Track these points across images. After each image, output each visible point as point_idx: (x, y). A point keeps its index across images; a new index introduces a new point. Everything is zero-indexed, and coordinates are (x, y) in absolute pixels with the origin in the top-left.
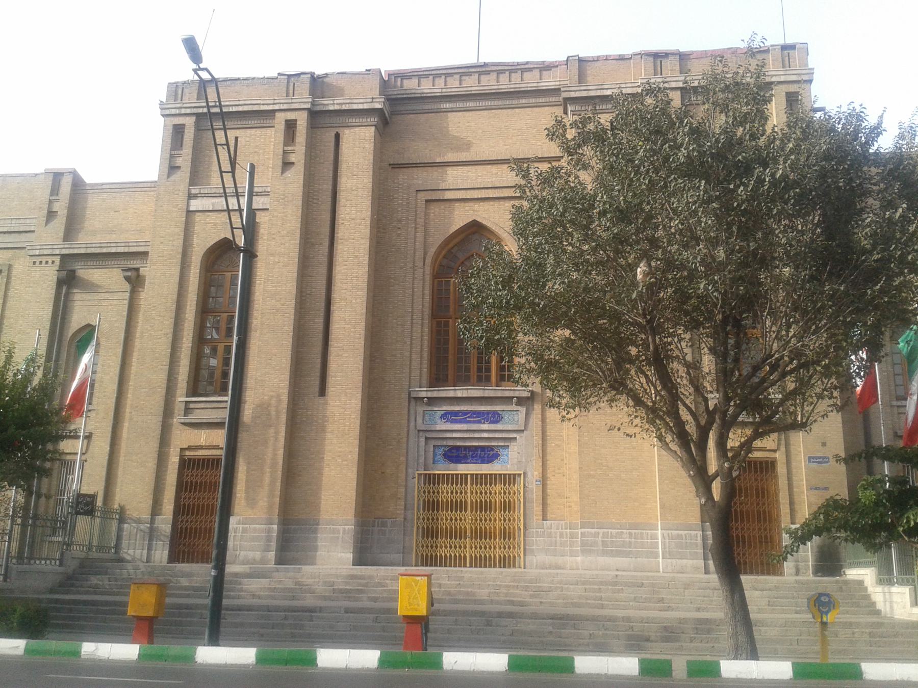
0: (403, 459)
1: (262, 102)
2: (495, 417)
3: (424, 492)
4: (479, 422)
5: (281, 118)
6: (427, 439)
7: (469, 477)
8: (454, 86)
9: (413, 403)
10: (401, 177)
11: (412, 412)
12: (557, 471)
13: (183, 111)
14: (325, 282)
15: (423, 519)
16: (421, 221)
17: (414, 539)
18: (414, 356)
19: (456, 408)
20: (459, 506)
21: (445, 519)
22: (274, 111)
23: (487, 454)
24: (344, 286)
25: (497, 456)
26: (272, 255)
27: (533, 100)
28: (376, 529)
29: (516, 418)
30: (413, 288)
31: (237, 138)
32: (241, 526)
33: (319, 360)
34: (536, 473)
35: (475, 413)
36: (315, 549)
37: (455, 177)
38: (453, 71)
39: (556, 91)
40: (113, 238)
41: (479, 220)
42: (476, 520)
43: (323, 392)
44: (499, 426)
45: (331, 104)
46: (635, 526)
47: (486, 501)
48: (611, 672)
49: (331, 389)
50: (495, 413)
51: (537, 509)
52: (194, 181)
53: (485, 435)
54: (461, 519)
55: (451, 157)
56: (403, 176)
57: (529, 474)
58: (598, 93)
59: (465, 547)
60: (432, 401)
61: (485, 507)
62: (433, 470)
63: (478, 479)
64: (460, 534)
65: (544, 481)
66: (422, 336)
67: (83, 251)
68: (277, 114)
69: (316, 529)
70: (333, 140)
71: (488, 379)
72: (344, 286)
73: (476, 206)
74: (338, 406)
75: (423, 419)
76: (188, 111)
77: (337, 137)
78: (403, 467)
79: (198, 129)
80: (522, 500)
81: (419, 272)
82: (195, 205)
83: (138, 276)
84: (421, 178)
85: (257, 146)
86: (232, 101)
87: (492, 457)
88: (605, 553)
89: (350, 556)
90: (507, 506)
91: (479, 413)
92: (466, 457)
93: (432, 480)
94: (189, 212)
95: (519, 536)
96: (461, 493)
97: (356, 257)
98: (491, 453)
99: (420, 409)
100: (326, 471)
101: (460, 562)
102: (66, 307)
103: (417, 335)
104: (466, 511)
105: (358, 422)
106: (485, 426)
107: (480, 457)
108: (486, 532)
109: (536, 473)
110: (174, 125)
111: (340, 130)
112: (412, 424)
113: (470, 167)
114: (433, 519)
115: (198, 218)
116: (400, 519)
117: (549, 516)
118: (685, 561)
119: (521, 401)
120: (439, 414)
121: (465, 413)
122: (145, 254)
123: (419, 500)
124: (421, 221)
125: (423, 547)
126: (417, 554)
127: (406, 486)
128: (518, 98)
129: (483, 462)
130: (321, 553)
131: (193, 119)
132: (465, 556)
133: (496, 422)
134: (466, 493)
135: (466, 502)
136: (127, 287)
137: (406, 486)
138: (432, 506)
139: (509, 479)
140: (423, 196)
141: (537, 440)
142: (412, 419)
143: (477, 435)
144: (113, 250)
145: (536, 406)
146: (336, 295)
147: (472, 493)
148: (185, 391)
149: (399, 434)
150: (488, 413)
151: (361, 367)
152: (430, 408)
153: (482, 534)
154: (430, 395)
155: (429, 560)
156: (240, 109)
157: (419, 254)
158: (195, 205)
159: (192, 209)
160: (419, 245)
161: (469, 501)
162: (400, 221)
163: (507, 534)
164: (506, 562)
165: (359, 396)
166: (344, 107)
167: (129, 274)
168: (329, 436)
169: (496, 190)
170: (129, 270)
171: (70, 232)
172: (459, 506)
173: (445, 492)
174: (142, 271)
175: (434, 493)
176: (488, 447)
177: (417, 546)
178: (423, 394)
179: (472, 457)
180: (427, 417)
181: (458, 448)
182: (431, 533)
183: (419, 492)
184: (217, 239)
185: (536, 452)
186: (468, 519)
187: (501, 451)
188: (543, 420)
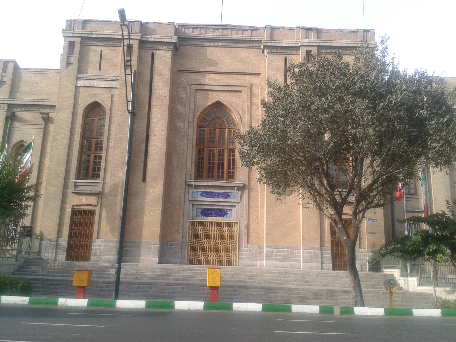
0: (182, 214)
1: (115, 34)
2: (226, 196)
3: (192, 230)
4: (219, 198)
6: (193, 204)
8: (210, 34)
9: (187, 187)
10: (183, 77)
11: (187, 191)
12: (255, 222)
13: (75, 35)
14: (146, 126)
15: (191, 242)
16: (193, 99)
17: (186, 252)
18: (188, 165)
19: (208, 191)
20: (208, 237)
21: (202, 242)
23: (221, 213)
24: (156, 129)
25: (226, 214)
27: (247, 45)
28: (168, 247)
29: (236, 196)
30: (188, 132)
31: (101, 51)
32: (103, 244)
33: (143, 165)
34: (245, 222)
35: (216, 193)
36: (140, 255)
37: (209, 79)
38: (210, 27)
39: (260, 42)
40: (35, 97)
41: (220, 100)
42: (216, 243)
43: (144, 180)
44: (228, 200)
45: (150, 38)
46: (290, 248)
47: (221, 235)
48: (307, 312)
49: (148, 179)
50: (226, 193)
51: (245, 239)
52: (79, 71)
53: (221, 204)
54: (209, 243)
55: (208, 69)
56: (184, 77)
57: (242, 223)
58: (280, 45)
59: (211, 256)
60: (197, 187)
61: (219, 237)
62: (196, 219)
63: (218, 224)
64: (208, 250)
65: (248, 226)
66: (192, 155)
67: (19, 103)
69: (140, 246)
70: (151, 56)
71: (222, 177)
72: (156, 129)
73: (219, 94)
74: (152, 187)
76: (77, 35)
77: (153, 54)
78: (182, 218)
79: (82, 45)
80: (238, 235)
81: (191, 124)
82: (80, 83)
83: (48, 117)
84: (193, 78)
86: (97, 32)
87: (224, 214)
88: (276, 260)
89: (157, 259)
90: (230, 237)
91: (219, 194)
92: (211, 214)
93: (195, 224)
94: (76, 86)
95: (236, 251)
96: (209, 230)
98: (224, 212)
99: (191, 190)
100: (145, 218)
101: (207, 262)
102: (10, 131)
103: (190, 154)
104: (211, 239)
105: (162, 195)
106: (221, 200)
108: (220, 249)
109: (245, 222)
110: (70, 42)
111: (154, 51)
112: (187, 197)
113: (217, 75)
114: (196, 243)
115: (81, 90)
116: (180, 242)
117: (250, 242)
118: (312, 264)
119: (239, 188)
120: (200, 193)
121: (212, 193)
122: (53, 107)
123: (189, 233)
124: (193, 99)
125: (190, 255)
126: (188, 259)
127: (183, 227)
128: (241, 43)
129: (219, 216)
130: (142, 258)
131: (80, 39)
132: (210, 260)
133: (227, 198)
134: (212, 231)
135: (211, 235)
136: (43, 122)
137: (183, 227)
138: (195, 236)
139: (231, 225)
140: (194, 87)
141: (246, 207)
142: (187, 195)
143: (217, 204)
144: (36, 103)
145: (245, 191)
146: (151, 133)
147: (214, 231)
148: (74, 177)
149: (180, 202)
150: (223, 193)
151: (163, 169)
152: (195, 190)
153: (218, 250)
154: (196, 184)
155: (192, 262)
156: (104, 36)
157: (192, 115)
158: (80, 83)
159: (78, 85)
160: (191, 111)
161: (213, 234)
162: (182, 98)
163: (229, 250)
164: (228, 263)
165: (162, 183)
166: (157, 40)
167: (44, 116)
168: (147, 201)
169: (229, 87)
170: (44, 114)
171: (12, 93)
172: (208, 237)
173: (201, 230)
174: (50, 115)
175: (196, 230)
176: (222, 209)
177: (188, 255)
178: (193, 183)
179: (214, 214)
180: (194, 194)
181: (208, 209)
182: (194, 249)
183: (189, 229)
184: (91, 101)
185: (245, 212)
186: (212, 243)
187: (228, 212)
188: (249, 198)
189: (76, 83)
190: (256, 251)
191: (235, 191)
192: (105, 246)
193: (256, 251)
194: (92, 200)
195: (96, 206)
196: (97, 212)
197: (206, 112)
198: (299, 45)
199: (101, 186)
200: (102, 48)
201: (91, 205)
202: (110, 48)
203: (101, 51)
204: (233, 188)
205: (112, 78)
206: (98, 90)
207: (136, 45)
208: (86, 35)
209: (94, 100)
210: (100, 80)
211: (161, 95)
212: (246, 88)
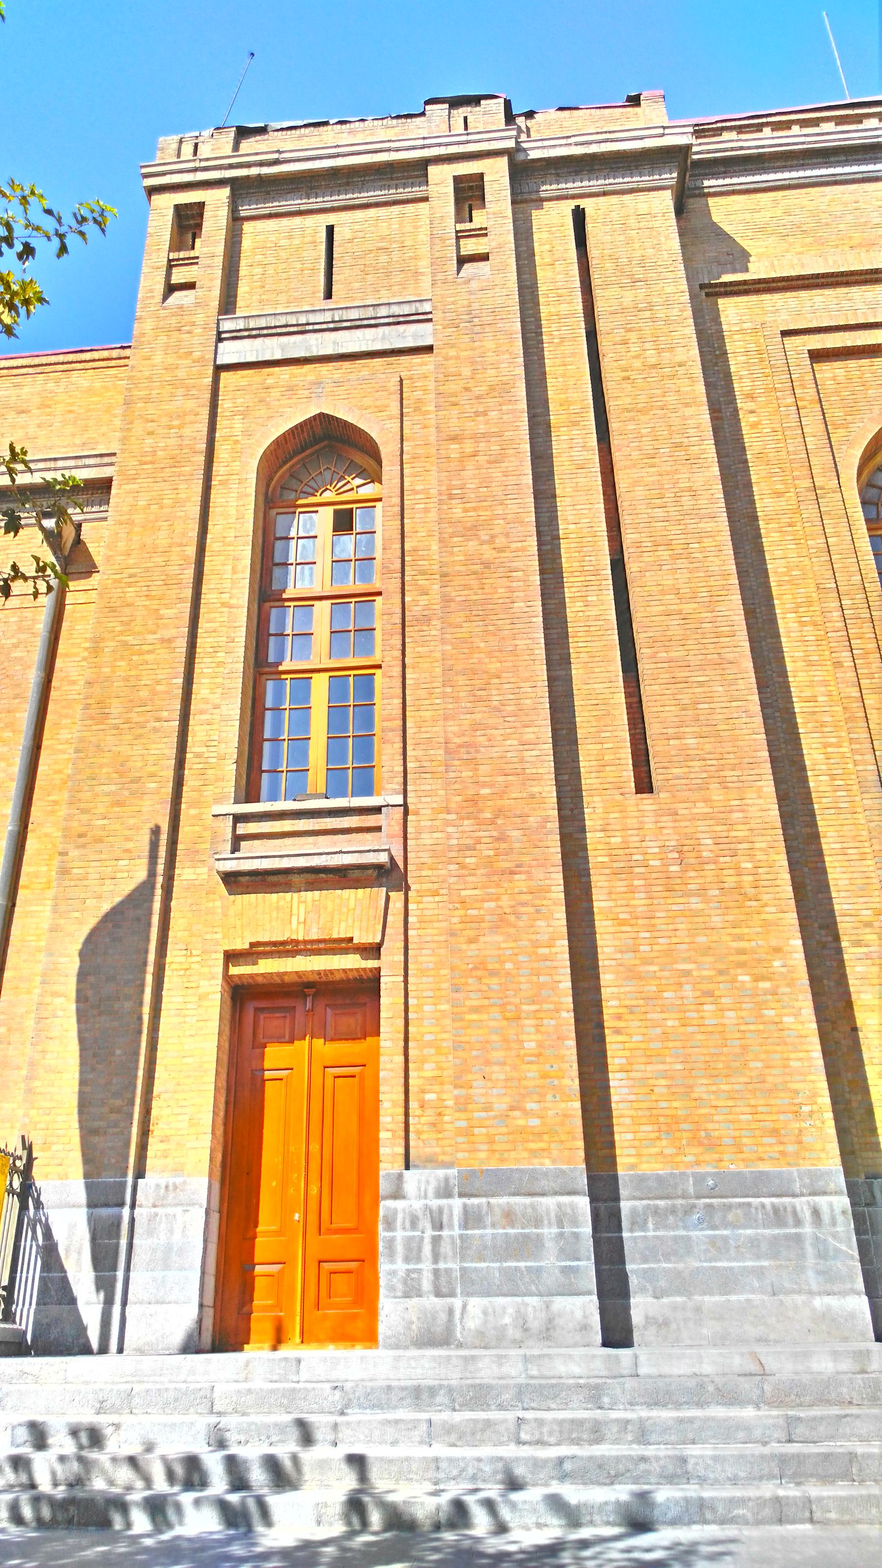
5: (441, 178)
22: (425, 163)
26: (454, 439)
31: (330, 230)
32: (457, 1204)
68: (432, 170)
74: (706, 817)
82: (230, 352)
85: (383, 238)
131: (226, 192)
148: (230, 787)
189: (218, 327)
192: (471, 1219)
194: (351, 913)
195: (374, 950)
196: (390, 983)
199: (390, 821)
200: (331, 219)
201: (344, 946)
202: (372, 212)
203: (330, 230)
205: (396, 310)
206: (324, 369)
207: (496, 175)
208: (254, 171)
209: (313, 412)
210: (337, 327)
211: (653, 361)
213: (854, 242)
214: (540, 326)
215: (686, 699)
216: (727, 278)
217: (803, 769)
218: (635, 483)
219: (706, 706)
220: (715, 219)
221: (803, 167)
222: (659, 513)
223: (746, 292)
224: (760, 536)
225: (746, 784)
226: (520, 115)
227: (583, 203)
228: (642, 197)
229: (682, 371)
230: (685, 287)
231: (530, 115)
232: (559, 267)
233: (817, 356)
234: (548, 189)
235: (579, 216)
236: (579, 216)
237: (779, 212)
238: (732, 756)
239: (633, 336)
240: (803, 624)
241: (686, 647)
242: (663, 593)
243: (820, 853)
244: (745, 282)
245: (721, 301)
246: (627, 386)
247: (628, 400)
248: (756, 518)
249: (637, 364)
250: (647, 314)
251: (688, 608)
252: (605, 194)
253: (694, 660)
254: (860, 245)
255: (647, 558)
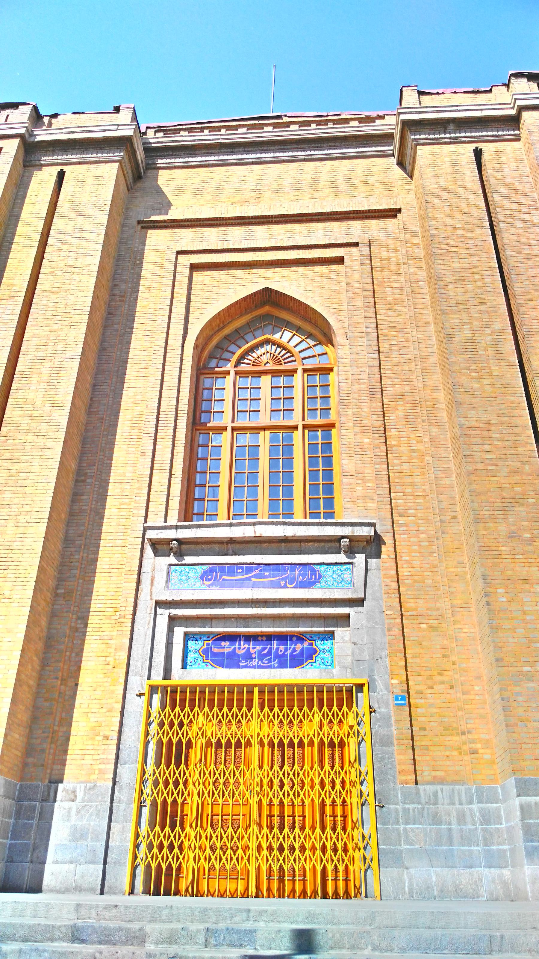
4: (276, 585)
6: (173, 621)
7: (256, 690)
25: (311, 653)
29: (347, 576)
63: (274, 697)
73: (270, 272)
75: (168, 580)
92: (248, 656)
97: (68, 314)
107: (277, 656)
119: (355, 545)
121: (250, 567)
129: (282, 665)
133: (310, 584)
180: (174, 576)
190: (461, 818)
191: (342, 558)
193: (461, 818)
197: (227, 331)
198: (513, 112)
204: (330, 544)
211: (71, 263)
212: (354, 249)
213: (235, 200)
214: (13, 239)
215: (14, 469)
216: (154, 218)
217: (102, 518)
218: (34, 336)
219: (25, 474)
220: (159, 182)
221: (218, 154)
222: (42, 354)
223: (166, 227)
224: (125, 373)
225: (30, 524)
226: (46, 116)
227: (65, 168)
228: (101, 166)
229: (86, 269)
230: (106, 221)
231: (55, 116)
232: (37, 206)
233: (194, 267)
234: (46, 159)
235: (61, 175)
236: (61, 175)
237: (197, 181)
238: (28, 506)
239: (65, 248)
240: (133, 428)
241: (26, 437)
242: (25, 403)
243: (94, 572)
244: (165, 221)
245: (150, 232)
246: (51, 277)
247: (48, 285)
248: (126, 362)
249: (62, 264)
250: (78, 235)
251: (36, 413)
252: (80, 163)
253: (28, 445)
254: (238, 202)
255: (24, 381)
